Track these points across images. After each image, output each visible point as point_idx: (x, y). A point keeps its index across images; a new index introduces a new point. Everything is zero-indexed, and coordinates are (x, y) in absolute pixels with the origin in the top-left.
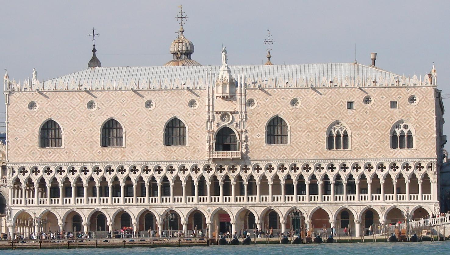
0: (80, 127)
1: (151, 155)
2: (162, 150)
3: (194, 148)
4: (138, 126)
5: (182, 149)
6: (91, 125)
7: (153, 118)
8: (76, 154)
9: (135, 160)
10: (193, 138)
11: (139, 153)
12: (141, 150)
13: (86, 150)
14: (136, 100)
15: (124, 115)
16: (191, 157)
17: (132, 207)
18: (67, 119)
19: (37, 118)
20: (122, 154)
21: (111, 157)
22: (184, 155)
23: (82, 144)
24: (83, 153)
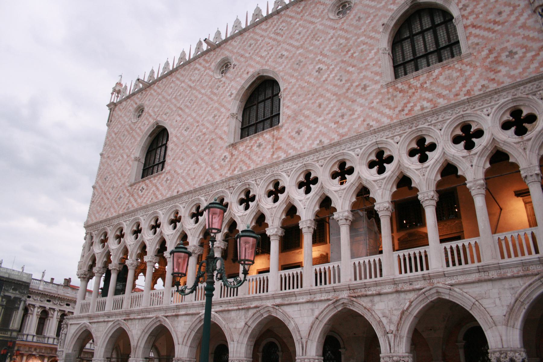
0: (198, 118)
1: (349, 124)
2: (380, 97)
3: (491, 51)
4: (315, 62)
5: (447, 72)
6: (216, 105)
7: (352, 29)
8: (183, 177)
9: (305, 149)
10: (480, 27)
11: (315, 130)
12: (322, 118)
13: (200, 162)
14: (310, 14)
15: (282, 55)
16: (486, 82)
17: (293, 300)
18: (180, 112)
19: (138, 131)
20: (273, 145)
21: (248, 162)
22: (460, 84)
23: (194, 153)
24: (194, 170)
